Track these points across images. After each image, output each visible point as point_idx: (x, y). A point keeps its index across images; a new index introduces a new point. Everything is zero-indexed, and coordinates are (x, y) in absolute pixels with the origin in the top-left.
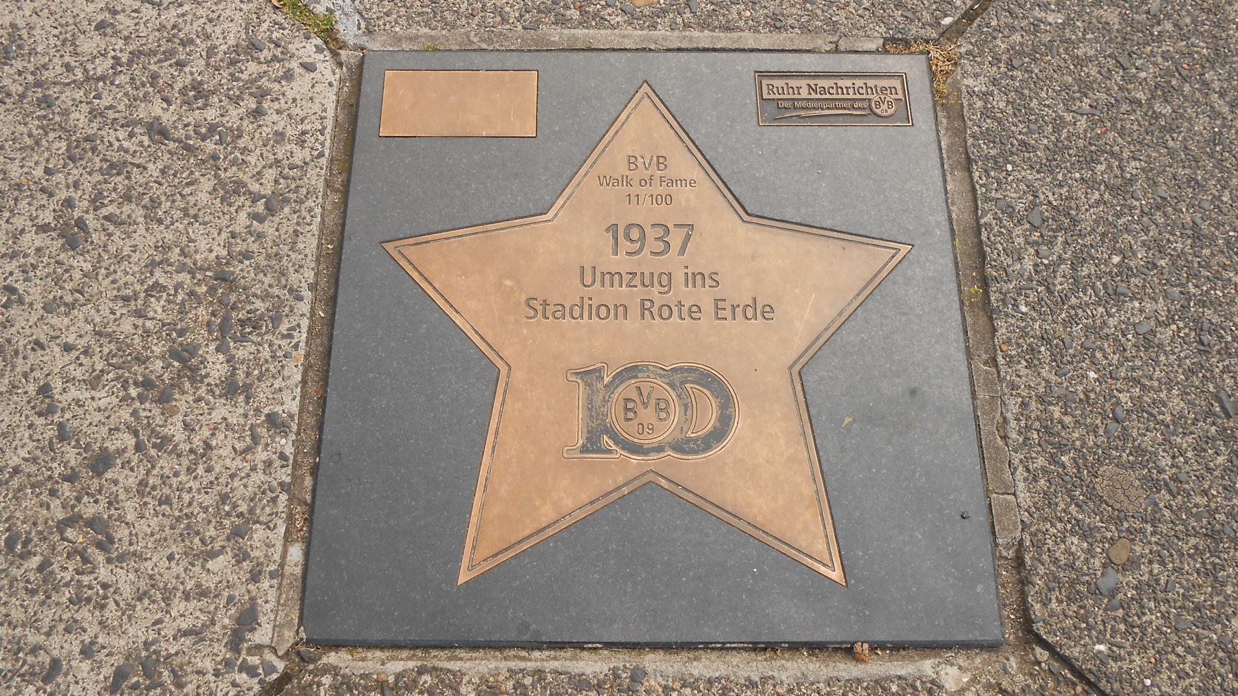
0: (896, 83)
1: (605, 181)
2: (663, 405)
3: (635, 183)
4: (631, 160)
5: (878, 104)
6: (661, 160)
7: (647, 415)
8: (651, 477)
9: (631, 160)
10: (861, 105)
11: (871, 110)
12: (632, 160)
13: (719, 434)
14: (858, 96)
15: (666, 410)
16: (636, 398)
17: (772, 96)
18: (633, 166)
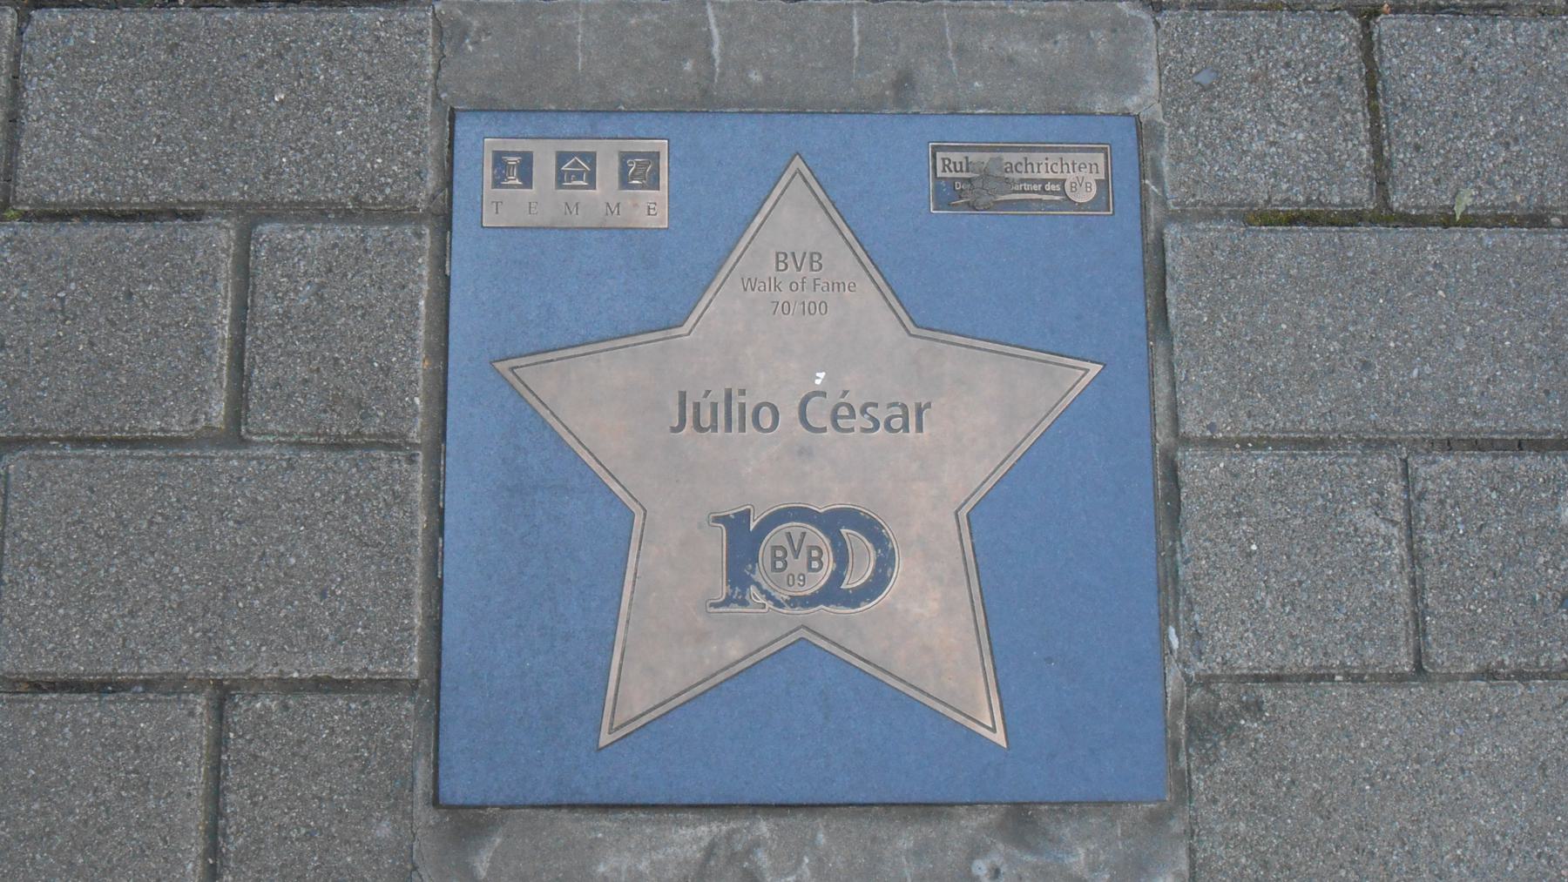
0: (1100, 158)
1: (750, 283)
2: (815, 553)
3: (785, 287)
4: (781, 258)
5: (1074, 188)
6: (816, 258)
7: (797, 565)
8: (804, 633)
9: (781, 258)
10: (1053, 188)
11: (1063, 192)
12: (782, 257)
13: (878, 583)
14: (1051, 176)
15: (819, 559)
16: (786, 545)
17: (948, 175)
18: (782, 266)
